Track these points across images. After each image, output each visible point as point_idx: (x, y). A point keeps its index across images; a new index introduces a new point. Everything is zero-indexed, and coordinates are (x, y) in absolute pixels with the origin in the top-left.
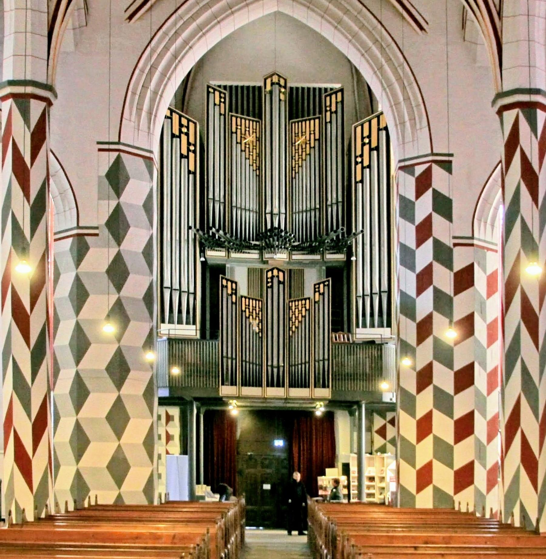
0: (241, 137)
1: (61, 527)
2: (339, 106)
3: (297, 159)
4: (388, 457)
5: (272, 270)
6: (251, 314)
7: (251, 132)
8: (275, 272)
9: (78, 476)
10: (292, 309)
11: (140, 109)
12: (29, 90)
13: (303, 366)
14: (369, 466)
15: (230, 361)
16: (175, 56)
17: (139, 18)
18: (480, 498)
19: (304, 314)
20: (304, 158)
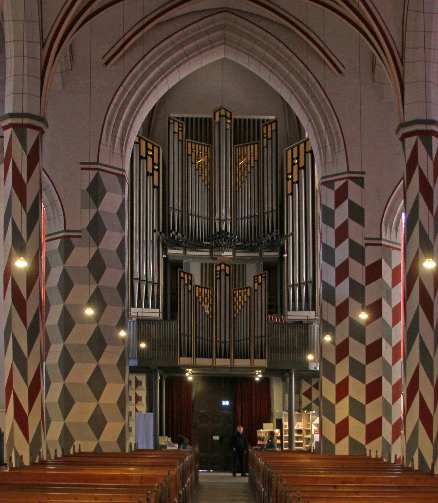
0: (195, 159)
1: (52, 470)
2: (274, 133)
3: (240, 176)
4: (313, 414)
5: (220, 265)
6: (203, 300)
7: (203, 154)
8: (223, 266)
9: (65, 429)
11: (114, 136)
12: (26, 121)
13: (245, 341)
14: (298, 421)
15: (186, 338)
16: (142, 94)
17: (114, 64)
18: (387, 447)
19: (245, 300)
20: (246, 175)
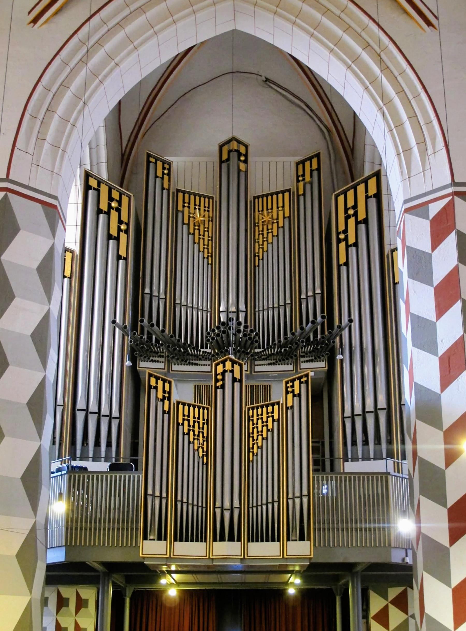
3: (261, 243)
8: (228, 365)
10: (253, 420)
11: (41, 139)
19: (270, 427)
20: (270, 241)
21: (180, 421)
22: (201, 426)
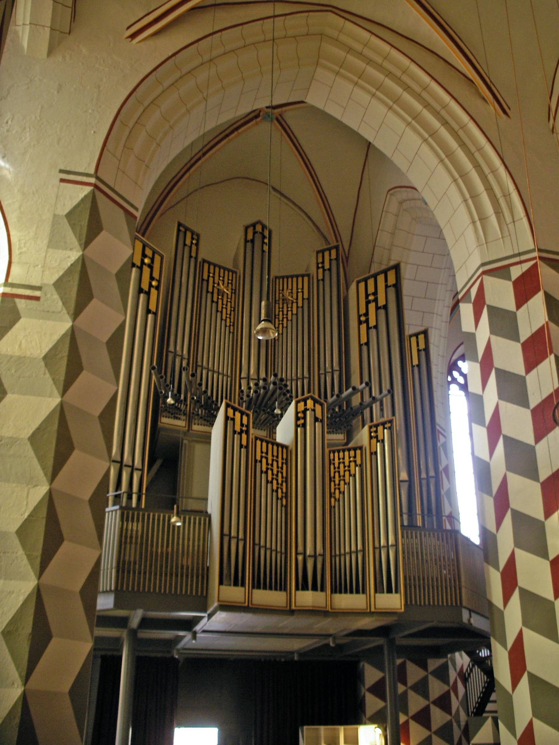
8: (310, 403)
20: (290, 318)
21: (258, 458)
22: (280, 465)
